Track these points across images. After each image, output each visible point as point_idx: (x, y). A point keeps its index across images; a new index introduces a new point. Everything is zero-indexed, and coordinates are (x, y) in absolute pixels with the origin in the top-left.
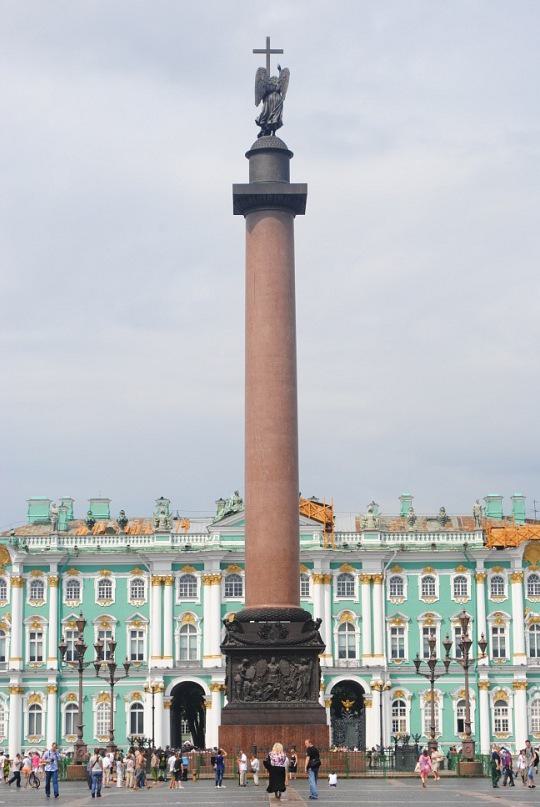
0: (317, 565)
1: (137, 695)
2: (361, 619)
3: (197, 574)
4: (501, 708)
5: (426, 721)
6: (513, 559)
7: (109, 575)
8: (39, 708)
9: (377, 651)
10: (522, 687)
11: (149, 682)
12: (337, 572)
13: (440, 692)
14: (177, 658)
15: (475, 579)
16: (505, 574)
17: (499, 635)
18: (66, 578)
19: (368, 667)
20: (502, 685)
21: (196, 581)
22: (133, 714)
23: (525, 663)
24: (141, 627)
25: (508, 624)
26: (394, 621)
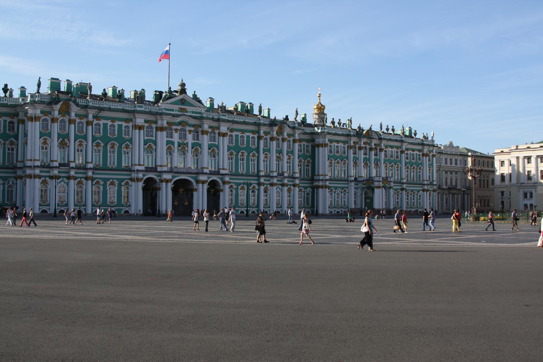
1: (127, 183)
3: (154, 126)
6: (273, 131)
7: (114, 122)
8: (81, 188)
11: (134, 175)
15: (259, 138)
16: (268, 137)
18: (95, 122)
19: (222, 175)
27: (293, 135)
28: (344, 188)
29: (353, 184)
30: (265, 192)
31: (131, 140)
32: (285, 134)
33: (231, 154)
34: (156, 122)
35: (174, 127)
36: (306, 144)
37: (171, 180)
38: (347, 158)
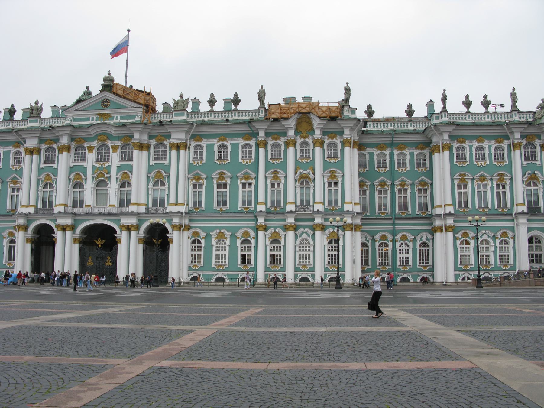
0: (136, 136)
1: (11, 234)
2: (169, 177)
3: (55, 146)
4: (276, 245)
5: (216, 255)
6: (287, 129)
9: (180, 201)
10: (291, 228)
12: (153, 142)
13: (227, 232)
14: (40, 206)
15: (258, 145)
16: (281, 142)
17: (276, 188)
20: (275, 228)
21: (55, 151)
22: (10, 247)
23: (294, 209)
24: (18, 185)
25: (283, 181)
26: (194, 178)
27: (342, 133)
28: (501, 228)
29: (523, 220)
30: (275, 241)
31: (20, 172)
32: (318, 133)
33: (198, 177)
34: (56, 141)
35: (86, 145)
36: (416, 152)
37: (73, 228)
38: (509, 167)
